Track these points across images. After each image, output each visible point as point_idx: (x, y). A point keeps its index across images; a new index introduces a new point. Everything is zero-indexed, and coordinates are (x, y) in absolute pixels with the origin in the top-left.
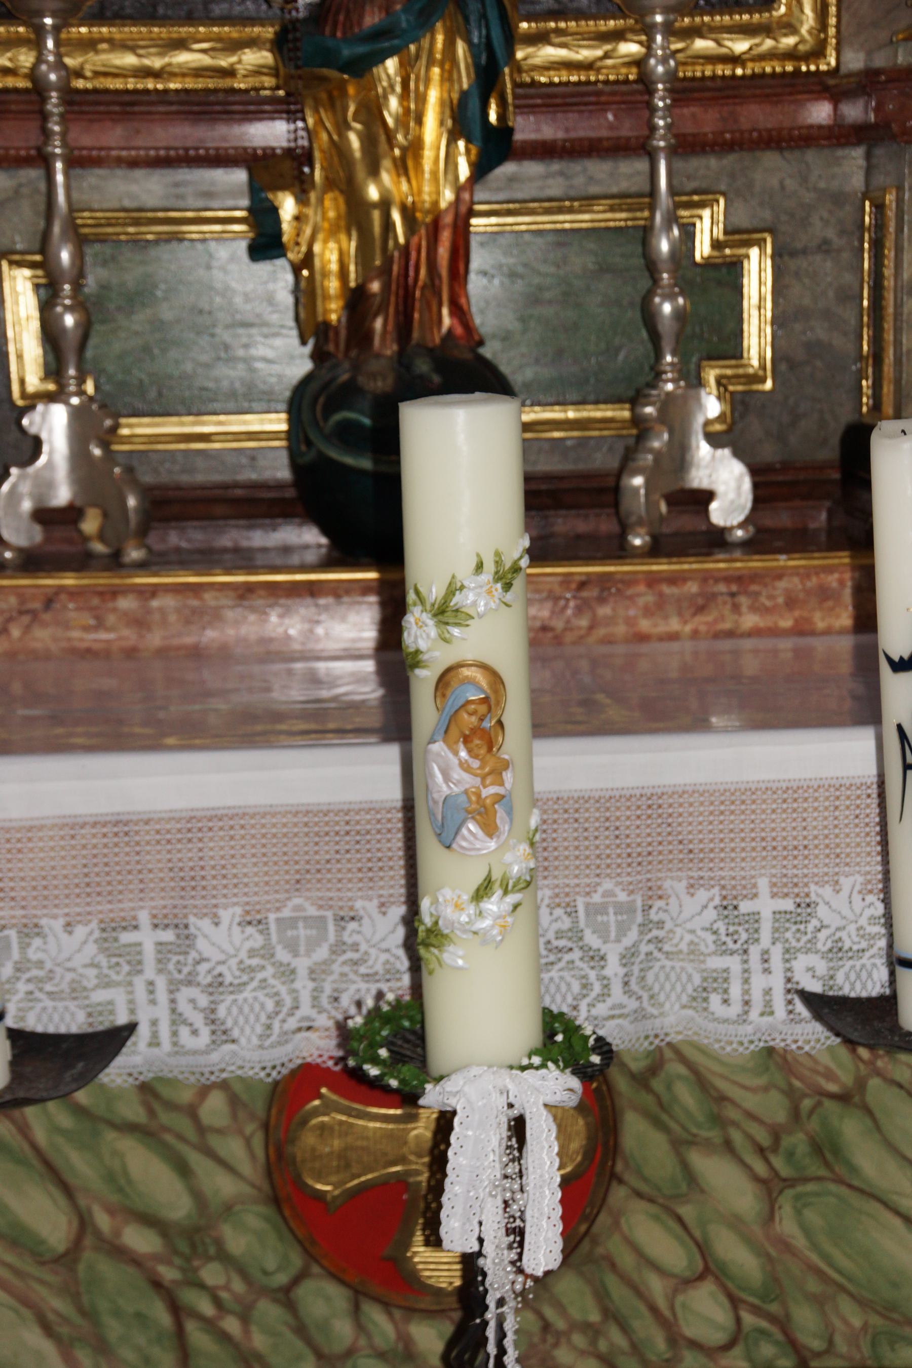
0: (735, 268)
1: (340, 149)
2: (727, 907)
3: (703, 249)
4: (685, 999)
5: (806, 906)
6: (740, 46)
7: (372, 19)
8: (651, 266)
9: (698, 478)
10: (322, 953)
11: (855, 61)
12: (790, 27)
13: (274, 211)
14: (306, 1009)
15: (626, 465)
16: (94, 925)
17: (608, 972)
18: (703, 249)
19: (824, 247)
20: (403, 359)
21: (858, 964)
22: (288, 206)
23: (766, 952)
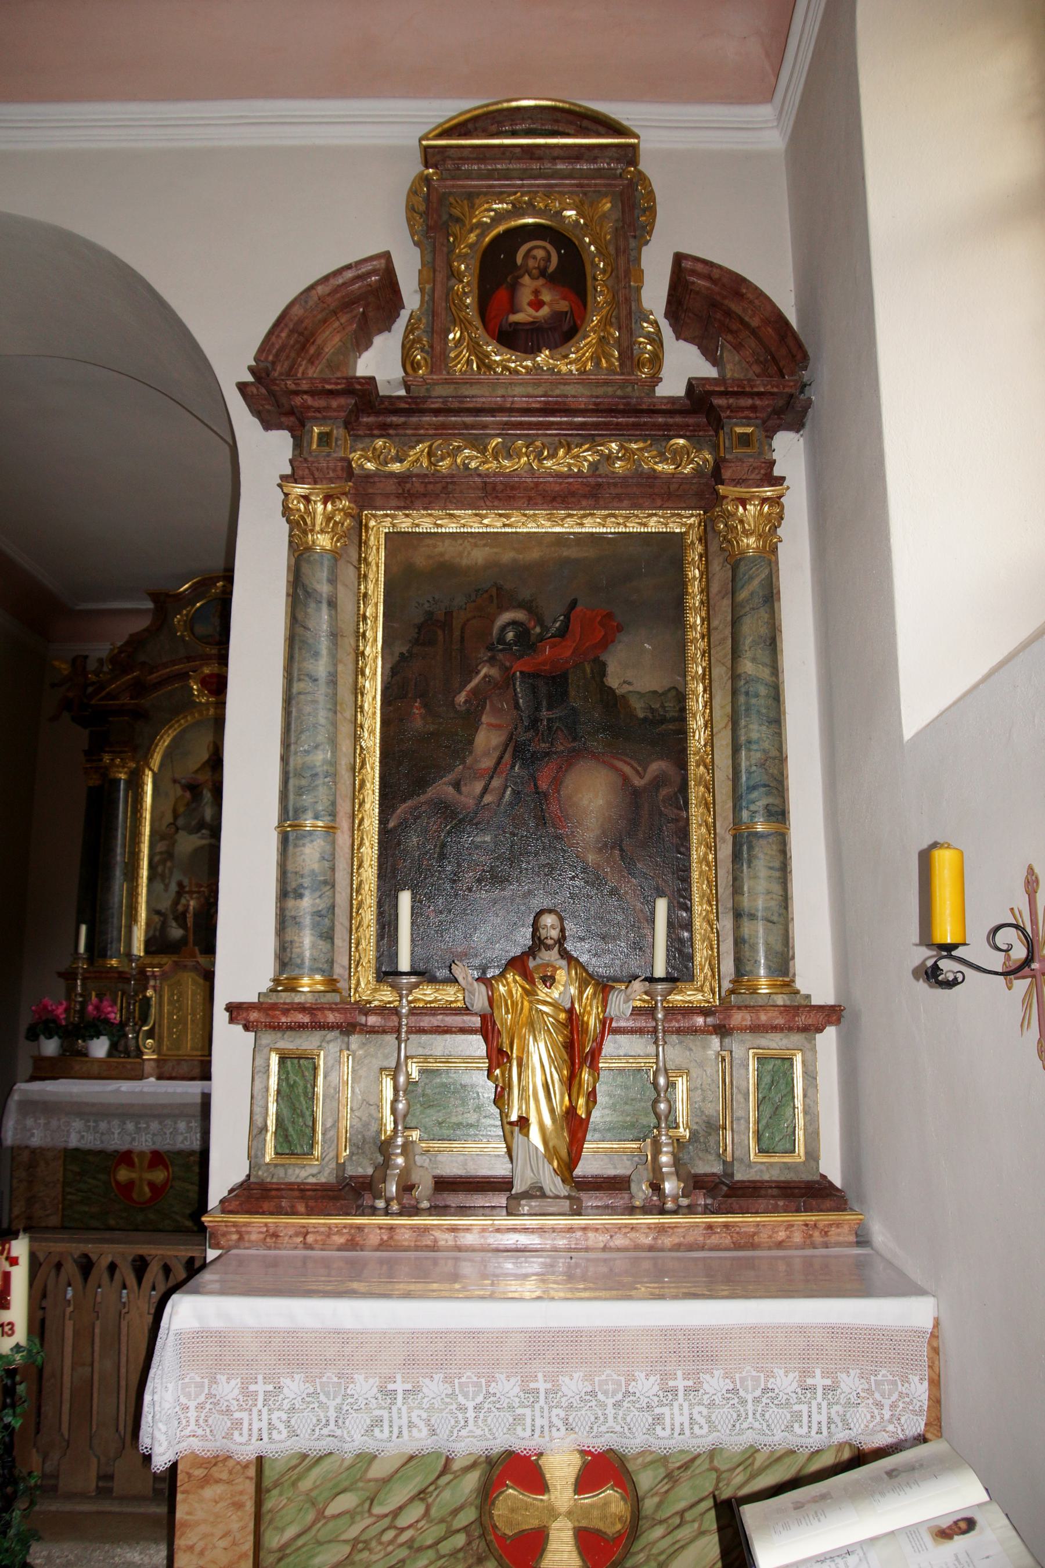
4: (644, 1431)
10: (339, 1400)
14: (192, 1426)
16: (239, 1380)
17: (329, 1414)
21: (579, 1413)
23: (681, 1405)
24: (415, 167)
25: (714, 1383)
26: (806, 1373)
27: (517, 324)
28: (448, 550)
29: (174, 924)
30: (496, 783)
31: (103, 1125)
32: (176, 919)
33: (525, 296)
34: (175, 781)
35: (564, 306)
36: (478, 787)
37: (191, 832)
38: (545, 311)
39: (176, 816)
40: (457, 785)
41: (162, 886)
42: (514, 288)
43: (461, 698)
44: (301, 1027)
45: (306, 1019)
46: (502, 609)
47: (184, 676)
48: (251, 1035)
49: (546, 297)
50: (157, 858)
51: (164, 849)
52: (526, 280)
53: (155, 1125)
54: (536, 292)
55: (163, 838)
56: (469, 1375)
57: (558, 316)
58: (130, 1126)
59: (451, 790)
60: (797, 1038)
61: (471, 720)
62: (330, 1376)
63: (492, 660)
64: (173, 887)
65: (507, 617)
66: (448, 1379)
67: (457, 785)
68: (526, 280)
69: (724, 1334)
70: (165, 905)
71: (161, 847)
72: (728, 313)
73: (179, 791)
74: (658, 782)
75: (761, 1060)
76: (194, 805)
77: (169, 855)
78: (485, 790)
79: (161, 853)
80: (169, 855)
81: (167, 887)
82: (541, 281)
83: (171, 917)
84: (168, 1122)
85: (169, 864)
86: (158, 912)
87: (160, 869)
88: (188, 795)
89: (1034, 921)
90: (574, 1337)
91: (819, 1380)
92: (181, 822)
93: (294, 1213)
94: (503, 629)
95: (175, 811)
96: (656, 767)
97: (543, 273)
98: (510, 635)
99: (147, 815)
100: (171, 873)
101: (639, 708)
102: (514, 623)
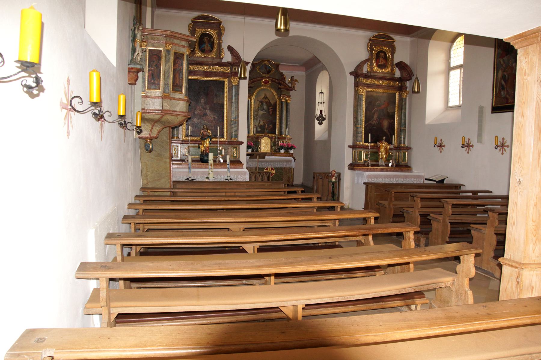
0: (222, 150)
1: (203, 143)
2: (221, 177)
3: (220, 149)
5: (224, 176)
6: (222, 139)
7: (205, 138)
8: (218, 150)
9: (220, 160)
11: (228, 141)
12: (225, 139)
13: (199, 146)
15: (217, 159)
18: (220, 149)
19: (227, 149)
20: (206, 153)
22: (200, 146)
24: (368, 41)
25: (408, 179)
26: (414, 179)
27: (380, 64)
28: (372, 93)
29: (259, 128)
30: (376, 121)
31: (263, 163)
32: (259, 127)
33: (381, 61)
34: (258, 101)
35: (385, 62)
36: (374, 122)
37: (261, 111)
38: (383, 63)
39: (258, 108)
40: (372, 121)
41: (256, 121)
42: (379, 59)
43: (373, 111)
44: (362, 148)
45: (362, 147)
46: (377, 101)
47: (261, 80)
48: (352, 149)
49: (383, 61)
50: (255, 115)
51: (256, 114)
52: (381, 58)
53: (272, 163)
54: (382, 60)
55: (256, 112)
56: (389, 179)
57: (384, 64)
58: (268, 163)
59: (372, 122)
60: (407, 151)
61: (374, 113)
62: (378, 179)
63: (376, 107)
64: (258, 121)
65: (378, 102)
66: (387, 179)
67: (372, 121)
68: (381, 58)
69: (408, 175)
70: (257, 124)
71: (256, 113)
72: (405, 68)
73: (259, 103)
74: (392, 122)
75: (403, 153)
76: (262, 106)
77: (257, 115)
78: (375, 122)
79: (256, 114)
80: (257, 115)
81: (257, 121)
82: (382, 59)
83: (258, 126)
84: (274, 163)
85: (257, 116)
86: (255, 126)
87: (256, 117)
88: (261, 103)
89: (441, 142)
90: (397, 175)
91: (415, 179)
92: (259, 109)
93: (361, 167)
94: (377, 104)
95: (258, 106)
96: (392, 120)
97: (383, 58)
98: (378, 104)
99: (253, 107)
100: (258, 118)
101: (391, 114)
102: (378, 103)
